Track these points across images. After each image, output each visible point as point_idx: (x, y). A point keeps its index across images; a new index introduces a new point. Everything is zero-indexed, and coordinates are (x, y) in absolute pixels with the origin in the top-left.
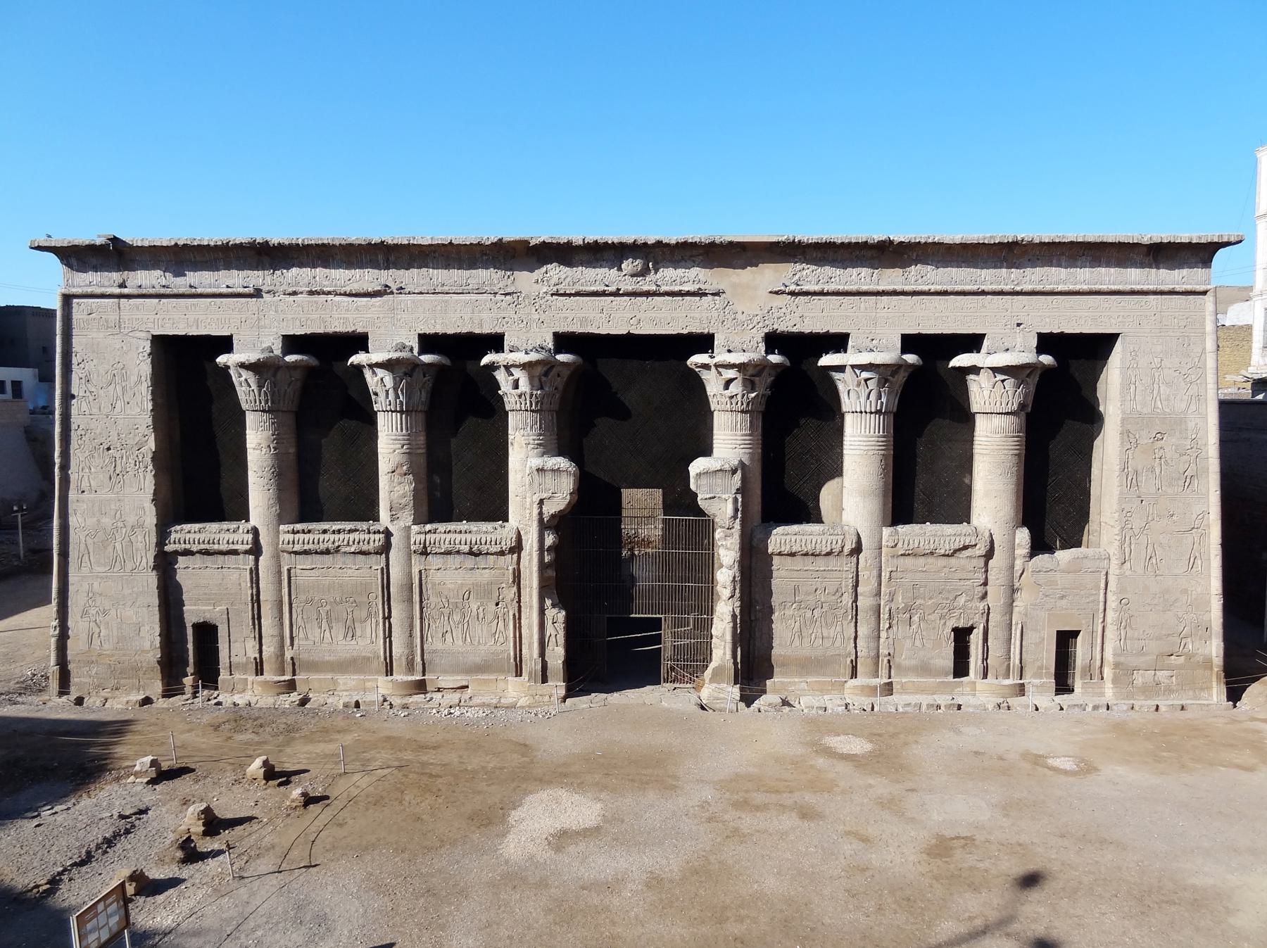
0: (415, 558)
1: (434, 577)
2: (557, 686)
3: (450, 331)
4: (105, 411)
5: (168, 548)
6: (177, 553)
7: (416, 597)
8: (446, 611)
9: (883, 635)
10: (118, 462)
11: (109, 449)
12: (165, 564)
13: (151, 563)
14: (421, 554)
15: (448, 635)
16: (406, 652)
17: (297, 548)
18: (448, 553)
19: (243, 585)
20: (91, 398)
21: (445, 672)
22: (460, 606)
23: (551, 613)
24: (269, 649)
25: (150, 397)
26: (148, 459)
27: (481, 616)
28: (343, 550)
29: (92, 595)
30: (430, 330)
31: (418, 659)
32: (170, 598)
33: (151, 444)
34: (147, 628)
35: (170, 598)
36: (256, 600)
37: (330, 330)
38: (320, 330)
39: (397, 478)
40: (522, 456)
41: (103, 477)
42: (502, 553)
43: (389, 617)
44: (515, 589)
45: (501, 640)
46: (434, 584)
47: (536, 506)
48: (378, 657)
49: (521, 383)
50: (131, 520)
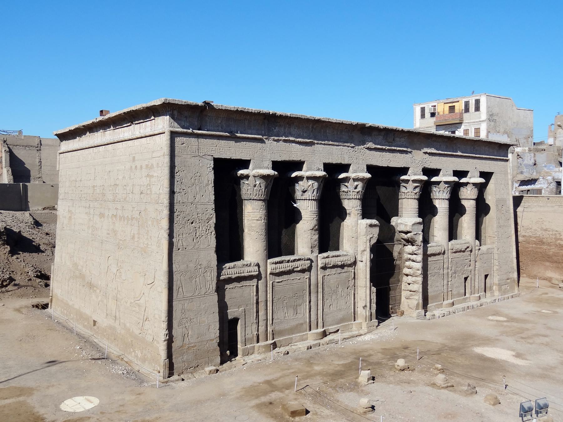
2: (375, 321)
3: (334, 163)
4: (190, 201)
5: (222, 278)
6: (230, 281)
7: (320, 290)
9: (450, 283)
10: (197, 231)
11: (192, 223)
12: (221, 287)
13: (214, 288)
17: (277, 271)
19: (252, 294)
20: (183, 193)
21: (330, 325)
23: (373, 288)
24: (262, 329)
25: (213, 193)
26: (213, 229)
28: (295, 270)
29: (183, 311)
30: (327, 161)
32: (223, 307)
33: (214, 220)
34: (213, 326)
35: (223, 307)
36: (257, 303)
37: (291, 159)
38: (287, 159)
39: (313, 232)
40: (356, 219)
41: (190, 240)
47: (368, 241)
48: (306, 322)
49: (359, 187)
50: (205, 264)
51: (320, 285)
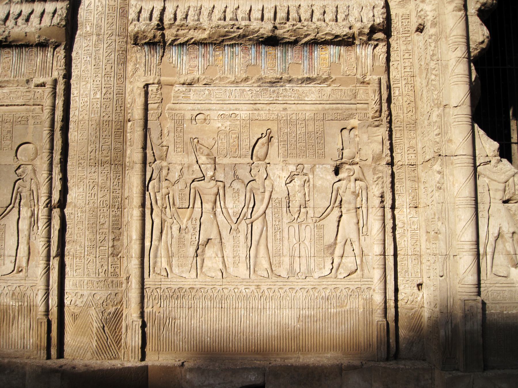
0: (139, 56)
1: (187, 103)
7: (134, 154)
8: (208, 187)
14: (152, 44)
15: (210, 252)
16: (102, 294)
18: (219, 41)
22: (244, 173)
27: (297, 201)
31: (131, 314)
42: (346, 41)
43: (62, 204)
44: (383, 131)
45: (349, 263)
46: (179, 122)
51: (135, 134)
